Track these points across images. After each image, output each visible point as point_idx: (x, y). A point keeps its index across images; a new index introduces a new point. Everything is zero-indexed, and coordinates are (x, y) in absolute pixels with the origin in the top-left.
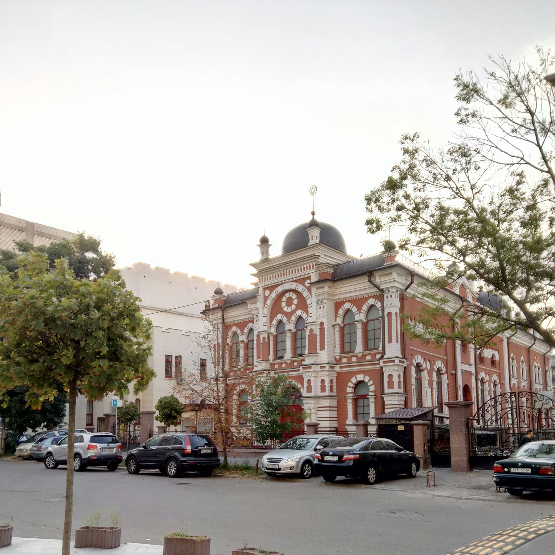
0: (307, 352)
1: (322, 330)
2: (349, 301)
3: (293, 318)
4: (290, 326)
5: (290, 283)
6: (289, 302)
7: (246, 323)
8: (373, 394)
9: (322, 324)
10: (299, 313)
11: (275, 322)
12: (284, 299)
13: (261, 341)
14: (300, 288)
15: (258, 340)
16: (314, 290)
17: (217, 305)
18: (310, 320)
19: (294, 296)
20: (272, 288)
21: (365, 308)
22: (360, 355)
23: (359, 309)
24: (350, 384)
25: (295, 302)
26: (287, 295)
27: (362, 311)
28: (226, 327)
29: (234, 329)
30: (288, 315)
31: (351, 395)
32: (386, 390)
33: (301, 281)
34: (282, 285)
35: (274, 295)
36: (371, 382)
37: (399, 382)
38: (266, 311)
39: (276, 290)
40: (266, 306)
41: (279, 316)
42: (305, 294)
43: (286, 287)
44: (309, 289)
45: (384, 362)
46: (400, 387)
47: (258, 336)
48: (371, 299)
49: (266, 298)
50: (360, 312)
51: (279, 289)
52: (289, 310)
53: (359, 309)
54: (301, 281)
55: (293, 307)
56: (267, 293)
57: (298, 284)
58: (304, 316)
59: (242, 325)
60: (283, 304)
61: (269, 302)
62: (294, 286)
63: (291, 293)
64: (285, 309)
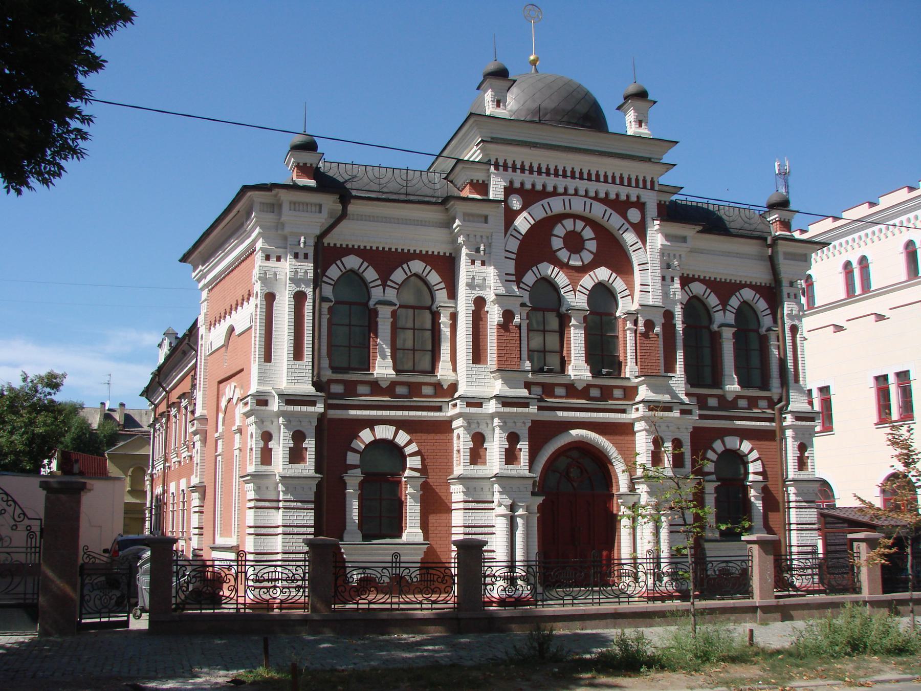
2: (703, 281)
3: (588, 281)
4: (577, 300)
5: (589, 201)
6: (574, 243)
7: (404, 257)
8: (760, 478)
9: (669, 316)
10: (603, 274)
12: (559, 230)
14: (614, 221)
16: (656, 237)
17: (312, 183)
19: (588, 233)
20: (531, 197)
21: (734, 302)
22: (730, 398)
23: (724, 303)
24: (711, 455)
25: (592, 245)
26: (569, 224)
27: (729, 308)
28: (324, 255)
29: (352, 262)
31: (713, 477)
32: (792, 472)
33: (620, 206)
34: (566, 198)
35: (539, 211)
36: (755, 455)
38: (514, 245)
39: (544, 202)
40: (511, 231)
42: (630, 238)
43: (578, 206)
45: (798, 419)
47: (480, 302)
48: (747, 289)
50: (724, 309)
51: (557, 205)
52: (575, 262)
53: (724, 303)
54: (620, 206)
55: (588, 257)
56: (516, 203)
57: (609, 211)
58: (619, 285)
59: (386, 261)
60: (557, 243)
62: (598, 211)
63: (580, 225)
64: (563, 255)
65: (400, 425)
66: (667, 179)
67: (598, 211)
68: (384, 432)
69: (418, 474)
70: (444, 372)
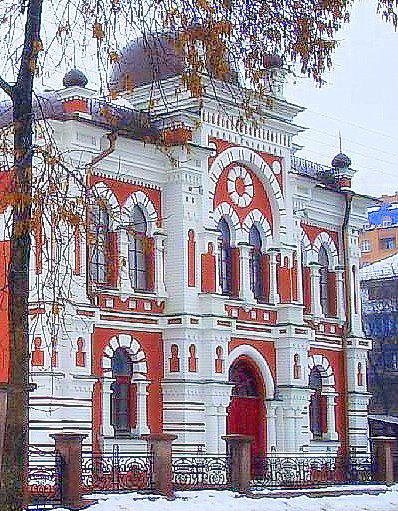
0: (275, 297)
1: (295, 262)
3: (248, 222)
10: (257, 214)
11: (217, 217)
12: (233, 175)
13: (201, 249)
14: (268, 173)
15: (192, 245)
17: (90, 118)
18: (283, 238)
19: (248, 180)
25: (250, 190)
30: (242, 212)
37: (360, 375)
41: (225, 207)
43: (247, 155)
44: (279, 177)
46: (360, 384)
49: (211, 160)
52: (242, 204)
54: (269, 158)
59: (123, 189)
60: (231, 186)
61: (217, 171)
64: (235, 197)
65: (134, 334)
66: (295, 140)
67: (259, 161)
68: (125, 340)
69: (145, 378)
70: (160, 292)
